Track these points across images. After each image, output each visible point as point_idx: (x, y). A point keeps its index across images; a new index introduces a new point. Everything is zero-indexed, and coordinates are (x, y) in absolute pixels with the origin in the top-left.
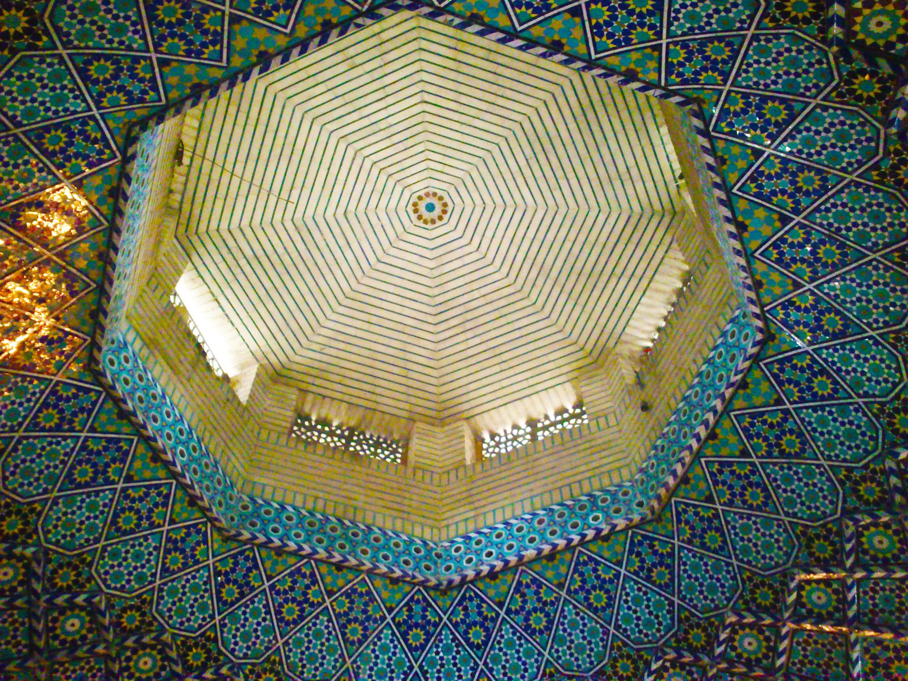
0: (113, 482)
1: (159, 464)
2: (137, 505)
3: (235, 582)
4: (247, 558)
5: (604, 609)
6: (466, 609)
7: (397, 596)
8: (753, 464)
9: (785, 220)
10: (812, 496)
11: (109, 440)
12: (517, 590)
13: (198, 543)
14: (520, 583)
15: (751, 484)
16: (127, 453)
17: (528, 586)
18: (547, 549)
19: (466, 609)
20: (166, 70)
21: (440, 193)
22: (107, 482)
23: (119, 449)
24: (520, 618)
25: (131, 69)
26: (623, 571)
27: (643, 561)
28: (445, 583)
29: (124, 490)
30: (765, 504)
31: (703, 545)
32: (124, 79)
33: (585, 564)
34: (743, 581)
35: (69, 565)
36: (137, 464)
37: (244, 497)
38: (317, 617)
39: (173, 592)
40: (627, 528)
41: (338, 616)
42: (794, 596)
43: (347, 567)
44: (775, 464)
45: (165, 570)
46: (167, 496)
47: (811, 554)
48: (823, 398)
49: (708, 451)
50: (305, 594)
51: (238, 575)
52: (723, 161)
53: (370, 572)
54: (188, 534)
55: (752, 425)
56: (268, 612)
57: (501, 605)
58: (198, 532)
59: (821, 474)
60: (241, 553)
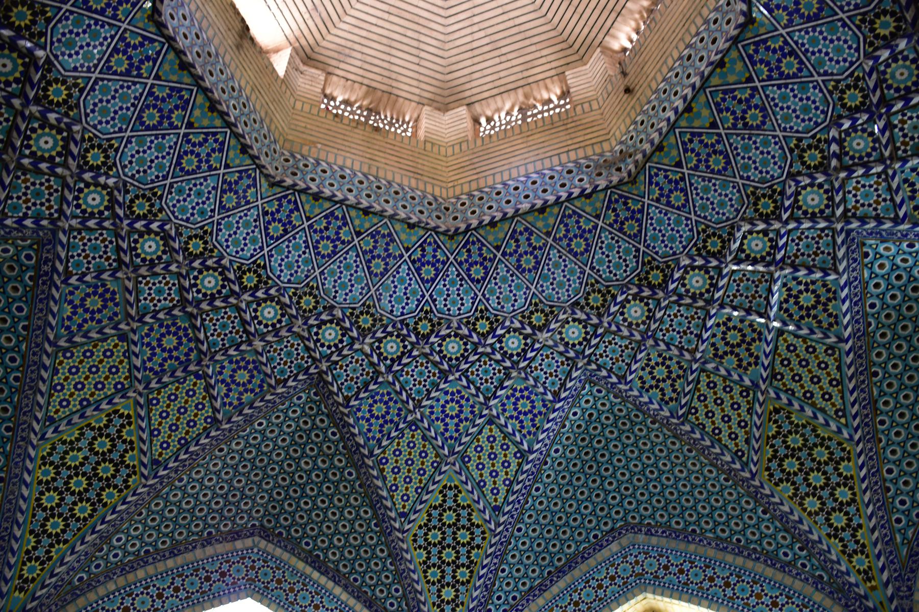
0: (176, 128)
1: (215, 114)
2: (197, 149)
3: (280, 221)
4: (289, 202)
5: (582, 254)
6: (469, 251)
7: (413, 237)
8: (719, 135)
10: (765, 163)
11: (172, 89)
12: (512, 237)
13: (249, 187)
14: (514, 231)
15: (715, 152)
17: (521, 233)
18: (539, 203)
19: (469, 251)
22: (172, 126)
23: (181, 97)
24: (513, 259)
26: (600, 223)
27: (617, 215)
28: (453, 229)
29: (186, 135)
30: (725, 169)
31: (668, 204)
33: (570, 216)
34: (698, 233)
35: (144, 196)
36: (197, 113)
37: (286, 153)
38: (347, 253)
39: (229, 226)
40: (607, 188)
41: (365, 253)
42: (738, 244)
43: (373, 213)
44: (738, 135)
46: (223, 143)
47: (756, 210)
48: (788, 77)
49: (683, 123)
50: (337, 233)
51: (282, 215)
53: (391, 217)
54: (240, 178)
55: (724, 100)
56: (307, 247)
57: (498, 248)
58: (249, 176)
59: (776, 143)
60: (285, 197)
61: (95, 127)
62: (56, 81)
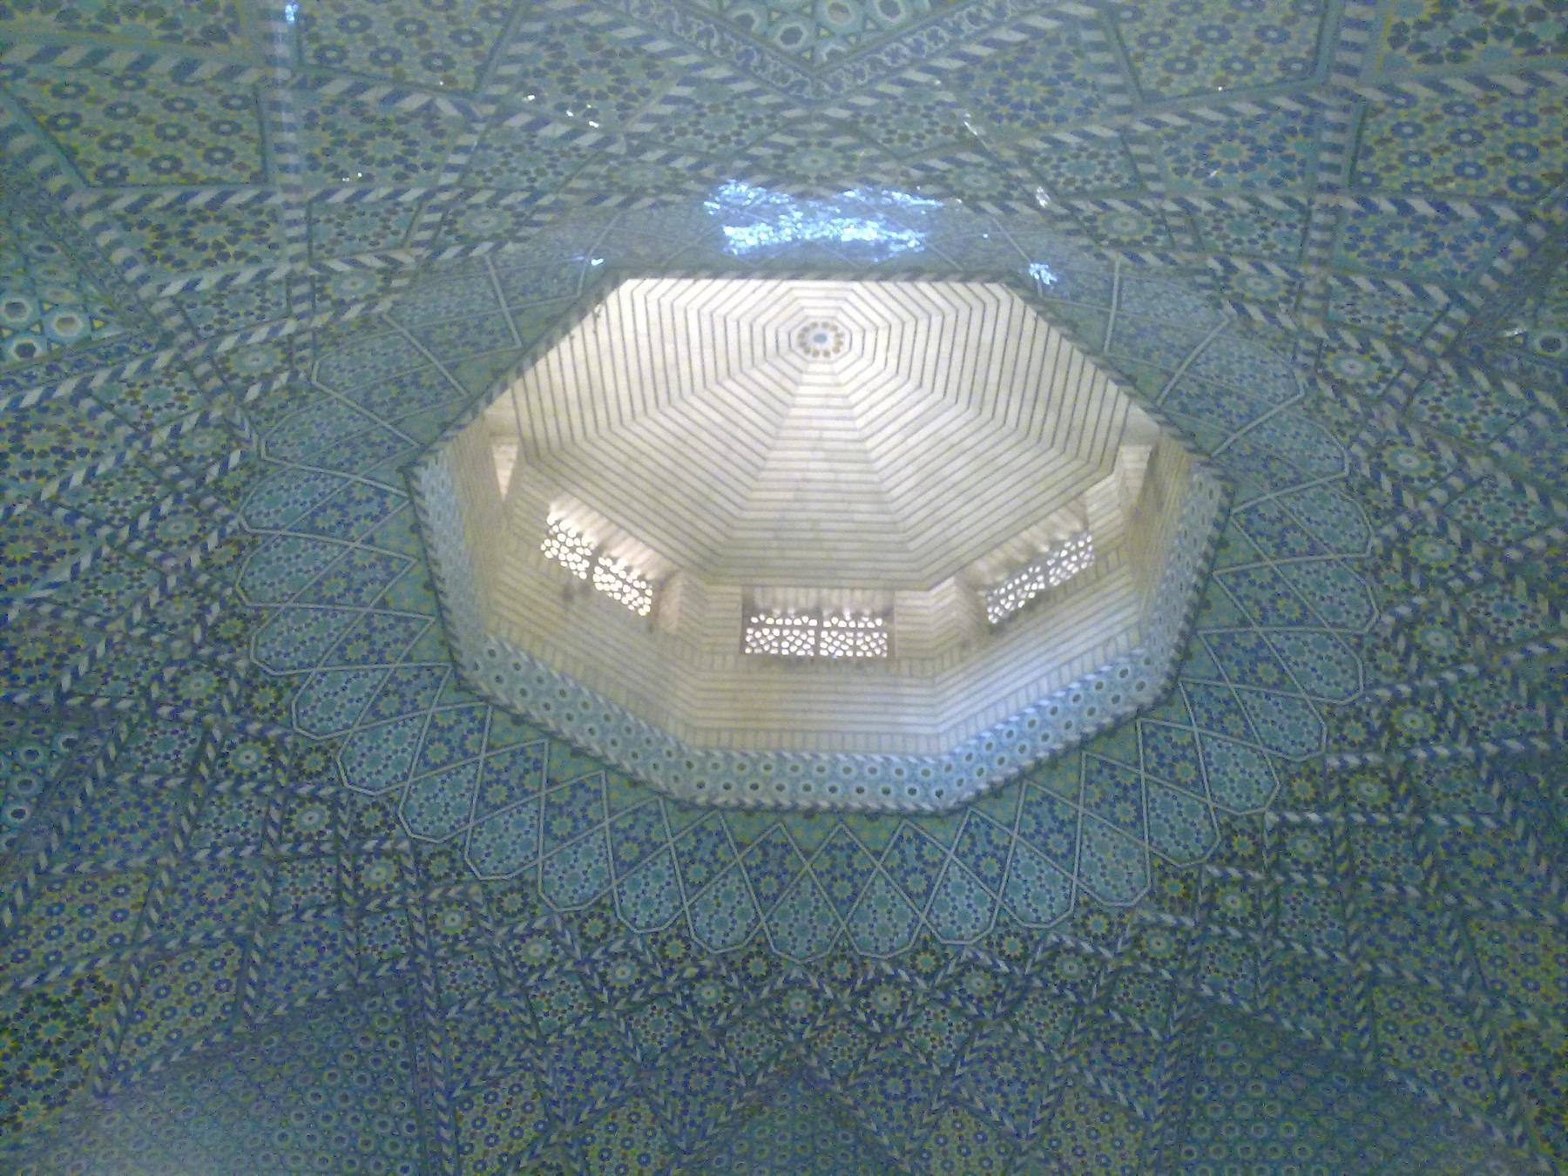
9: (383, 604)
16: (1221, 636)
20: (880, 847)
21: (800, 351)
22: (1261, 645)
25: (900, 867)
32: (913, 862)
52: (442, 643)
58: (1249, 521)
61: (1319, 739)
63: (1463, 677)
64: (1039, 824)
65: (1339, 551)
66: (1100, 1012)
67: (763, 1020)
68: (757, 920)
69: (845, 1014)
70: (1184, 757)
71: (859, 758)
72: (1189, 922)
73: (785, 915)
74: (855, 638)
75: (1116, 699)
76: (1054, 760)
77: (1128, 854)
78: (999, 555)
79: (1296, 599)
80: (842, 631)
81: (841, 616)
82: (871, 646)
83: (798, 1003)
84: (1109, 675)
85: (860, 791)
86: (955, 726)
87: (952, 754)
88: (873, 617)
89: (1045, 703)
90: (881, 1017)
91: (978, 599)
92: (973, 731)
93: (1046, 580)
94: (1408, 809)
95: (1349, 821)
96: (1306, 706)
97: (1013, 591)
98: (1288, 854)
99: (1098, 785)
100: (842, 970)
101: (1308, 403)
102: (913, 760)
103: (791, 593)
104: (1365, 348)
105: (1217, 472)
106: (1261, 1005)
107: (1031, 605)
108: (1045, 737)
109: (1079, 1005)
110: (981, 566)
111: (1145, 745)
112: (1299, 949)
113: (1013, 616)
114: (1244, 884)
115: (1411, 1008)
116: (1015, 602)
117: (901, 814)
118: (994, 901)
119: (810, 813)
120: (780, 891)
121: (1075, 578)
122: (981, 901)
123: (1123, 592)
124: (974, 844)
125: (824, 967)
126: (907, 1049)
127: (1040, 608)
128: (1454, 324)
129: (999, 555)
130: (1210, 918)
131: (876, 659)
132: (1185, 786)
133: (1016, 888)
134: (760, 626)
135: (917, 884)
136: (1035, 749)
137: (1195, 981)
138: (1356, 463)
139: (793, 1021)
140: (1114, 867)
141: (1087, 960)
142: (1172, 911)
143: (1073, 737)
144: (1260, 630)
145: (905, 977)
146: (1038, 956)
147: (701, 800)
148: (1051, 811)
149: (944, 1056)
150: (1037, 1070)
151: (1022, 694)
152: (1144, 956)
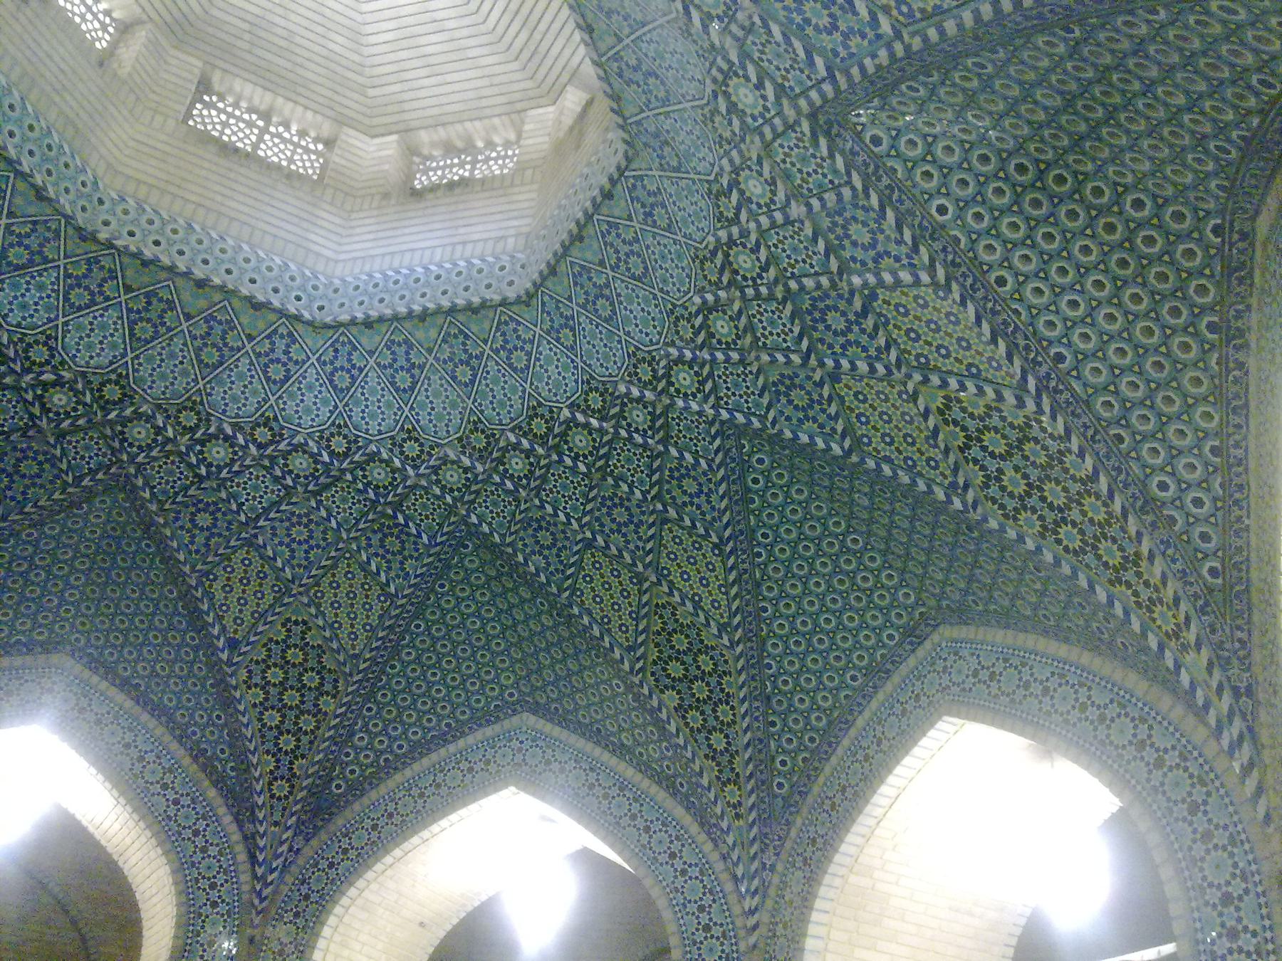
16: (582, 267)
20: (254, 333)
22: (607, 285)
25: (267, 355)
29: (612, 269)
32: (279, 354)
45: (669, 228)
58: (634, 186)
62: (586, 401)
63: (728, 360)
64: (395, 360)
65: (685, 236)
66: (390, 511)
67: (105, 437)
68: (124, 355)
69: (180, 454)
70: (522, 349)
71: (262, 254)
72: (480, 468)
73: (150, 359)
74: (294, 152)
75: (488, 286)
76: (424, 316)
77: (454, 405)
78: (442, 133)
79: (644, 262)
80: (284, 141)
81: (288, 128)
82: (306, 164)
83: (140, 432)
84: (491, 266)
85: (253, 281)
86: (355, 259)
87: (343, 281)
88: (316, 140)
89: (433, 268)
90: (210, 465)
91: (412, 163)
92: (367, 268)
93: (472, 171)
94: (657, 438)
95: (617, 433)
96: (620, 342)
97: (443, 168)
98: (566, 442)
99: (451, 346)
100: (189, 419)
101: (706, 110)
102: (308, 273)
103: (248, 89)
104: (759, 86)
105: (626, 136)
106: (508, 540)
107: (452, 185)
108: (423, 295)
109: (375, 503)
110: (424, 136)
111: (498, 329)
112: (549, 509)
113: (434, 188)
114: (528, 453)
115: (606, 571)
116: (443, 176)
117: (282, 313)
118: (336, 407)
119: (201, 284)
120: (153, 339)
121: (494, 177)
122: (325, 402)
123: (526, 205)
124: (336, 358)
125: (172, 411)
126: (223, 495)
127: (457, 191)
128: (822, 95)
129: (442, 133)
130: (495, 470)
131: (308, 177)
132: (515, 370)
133: (357, 403)
134: (209, 106)
135: (276, 372)
136: (412, 300)
137: (468, 511)
138: (720, 174)
139: (131, 445)
140: (440, 409)
141: (393, 471)
142: (470, 456)
143: (446, 304)
144: (611, 274)
145: (241, 441)
146: (356, 458)
147: (103, 236)
148: (407, 353)
149: (252, 509)
150: (325, 539)
151: (418, 255)
152: (438, 481)
